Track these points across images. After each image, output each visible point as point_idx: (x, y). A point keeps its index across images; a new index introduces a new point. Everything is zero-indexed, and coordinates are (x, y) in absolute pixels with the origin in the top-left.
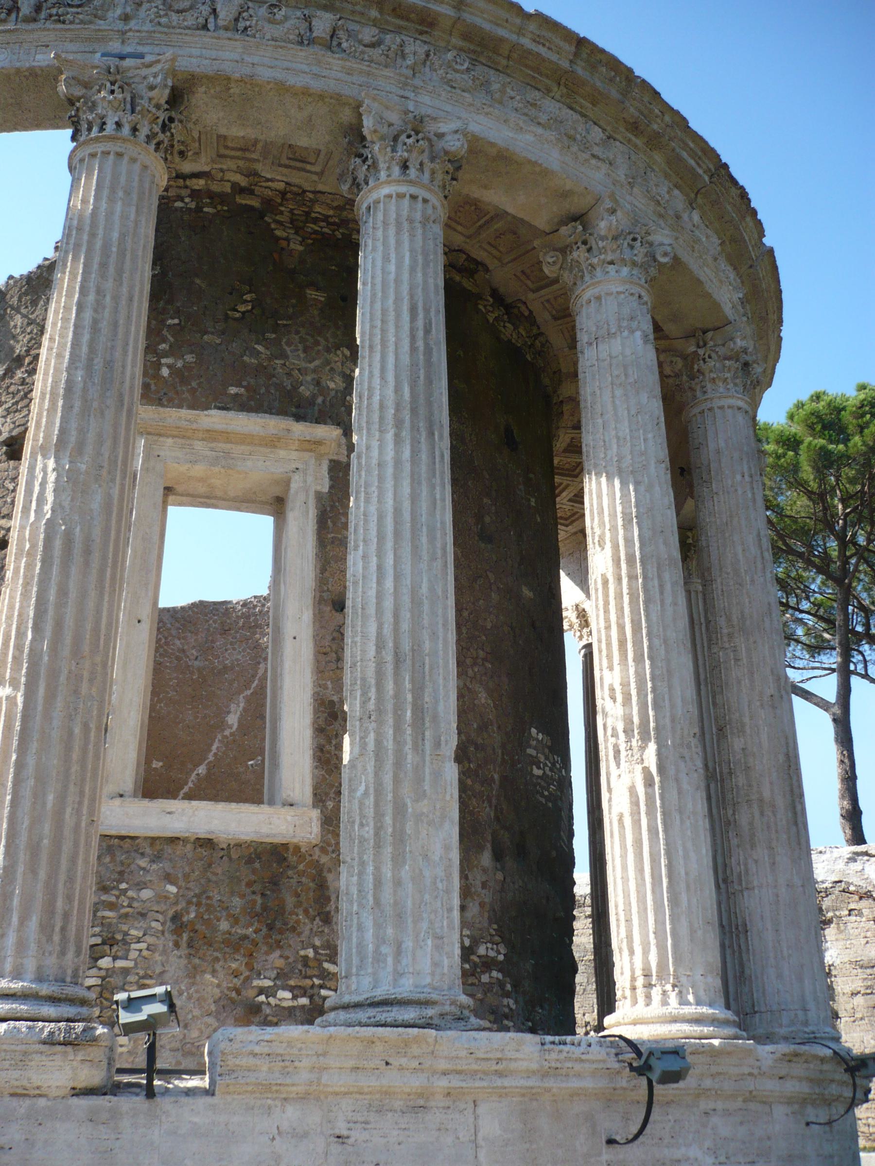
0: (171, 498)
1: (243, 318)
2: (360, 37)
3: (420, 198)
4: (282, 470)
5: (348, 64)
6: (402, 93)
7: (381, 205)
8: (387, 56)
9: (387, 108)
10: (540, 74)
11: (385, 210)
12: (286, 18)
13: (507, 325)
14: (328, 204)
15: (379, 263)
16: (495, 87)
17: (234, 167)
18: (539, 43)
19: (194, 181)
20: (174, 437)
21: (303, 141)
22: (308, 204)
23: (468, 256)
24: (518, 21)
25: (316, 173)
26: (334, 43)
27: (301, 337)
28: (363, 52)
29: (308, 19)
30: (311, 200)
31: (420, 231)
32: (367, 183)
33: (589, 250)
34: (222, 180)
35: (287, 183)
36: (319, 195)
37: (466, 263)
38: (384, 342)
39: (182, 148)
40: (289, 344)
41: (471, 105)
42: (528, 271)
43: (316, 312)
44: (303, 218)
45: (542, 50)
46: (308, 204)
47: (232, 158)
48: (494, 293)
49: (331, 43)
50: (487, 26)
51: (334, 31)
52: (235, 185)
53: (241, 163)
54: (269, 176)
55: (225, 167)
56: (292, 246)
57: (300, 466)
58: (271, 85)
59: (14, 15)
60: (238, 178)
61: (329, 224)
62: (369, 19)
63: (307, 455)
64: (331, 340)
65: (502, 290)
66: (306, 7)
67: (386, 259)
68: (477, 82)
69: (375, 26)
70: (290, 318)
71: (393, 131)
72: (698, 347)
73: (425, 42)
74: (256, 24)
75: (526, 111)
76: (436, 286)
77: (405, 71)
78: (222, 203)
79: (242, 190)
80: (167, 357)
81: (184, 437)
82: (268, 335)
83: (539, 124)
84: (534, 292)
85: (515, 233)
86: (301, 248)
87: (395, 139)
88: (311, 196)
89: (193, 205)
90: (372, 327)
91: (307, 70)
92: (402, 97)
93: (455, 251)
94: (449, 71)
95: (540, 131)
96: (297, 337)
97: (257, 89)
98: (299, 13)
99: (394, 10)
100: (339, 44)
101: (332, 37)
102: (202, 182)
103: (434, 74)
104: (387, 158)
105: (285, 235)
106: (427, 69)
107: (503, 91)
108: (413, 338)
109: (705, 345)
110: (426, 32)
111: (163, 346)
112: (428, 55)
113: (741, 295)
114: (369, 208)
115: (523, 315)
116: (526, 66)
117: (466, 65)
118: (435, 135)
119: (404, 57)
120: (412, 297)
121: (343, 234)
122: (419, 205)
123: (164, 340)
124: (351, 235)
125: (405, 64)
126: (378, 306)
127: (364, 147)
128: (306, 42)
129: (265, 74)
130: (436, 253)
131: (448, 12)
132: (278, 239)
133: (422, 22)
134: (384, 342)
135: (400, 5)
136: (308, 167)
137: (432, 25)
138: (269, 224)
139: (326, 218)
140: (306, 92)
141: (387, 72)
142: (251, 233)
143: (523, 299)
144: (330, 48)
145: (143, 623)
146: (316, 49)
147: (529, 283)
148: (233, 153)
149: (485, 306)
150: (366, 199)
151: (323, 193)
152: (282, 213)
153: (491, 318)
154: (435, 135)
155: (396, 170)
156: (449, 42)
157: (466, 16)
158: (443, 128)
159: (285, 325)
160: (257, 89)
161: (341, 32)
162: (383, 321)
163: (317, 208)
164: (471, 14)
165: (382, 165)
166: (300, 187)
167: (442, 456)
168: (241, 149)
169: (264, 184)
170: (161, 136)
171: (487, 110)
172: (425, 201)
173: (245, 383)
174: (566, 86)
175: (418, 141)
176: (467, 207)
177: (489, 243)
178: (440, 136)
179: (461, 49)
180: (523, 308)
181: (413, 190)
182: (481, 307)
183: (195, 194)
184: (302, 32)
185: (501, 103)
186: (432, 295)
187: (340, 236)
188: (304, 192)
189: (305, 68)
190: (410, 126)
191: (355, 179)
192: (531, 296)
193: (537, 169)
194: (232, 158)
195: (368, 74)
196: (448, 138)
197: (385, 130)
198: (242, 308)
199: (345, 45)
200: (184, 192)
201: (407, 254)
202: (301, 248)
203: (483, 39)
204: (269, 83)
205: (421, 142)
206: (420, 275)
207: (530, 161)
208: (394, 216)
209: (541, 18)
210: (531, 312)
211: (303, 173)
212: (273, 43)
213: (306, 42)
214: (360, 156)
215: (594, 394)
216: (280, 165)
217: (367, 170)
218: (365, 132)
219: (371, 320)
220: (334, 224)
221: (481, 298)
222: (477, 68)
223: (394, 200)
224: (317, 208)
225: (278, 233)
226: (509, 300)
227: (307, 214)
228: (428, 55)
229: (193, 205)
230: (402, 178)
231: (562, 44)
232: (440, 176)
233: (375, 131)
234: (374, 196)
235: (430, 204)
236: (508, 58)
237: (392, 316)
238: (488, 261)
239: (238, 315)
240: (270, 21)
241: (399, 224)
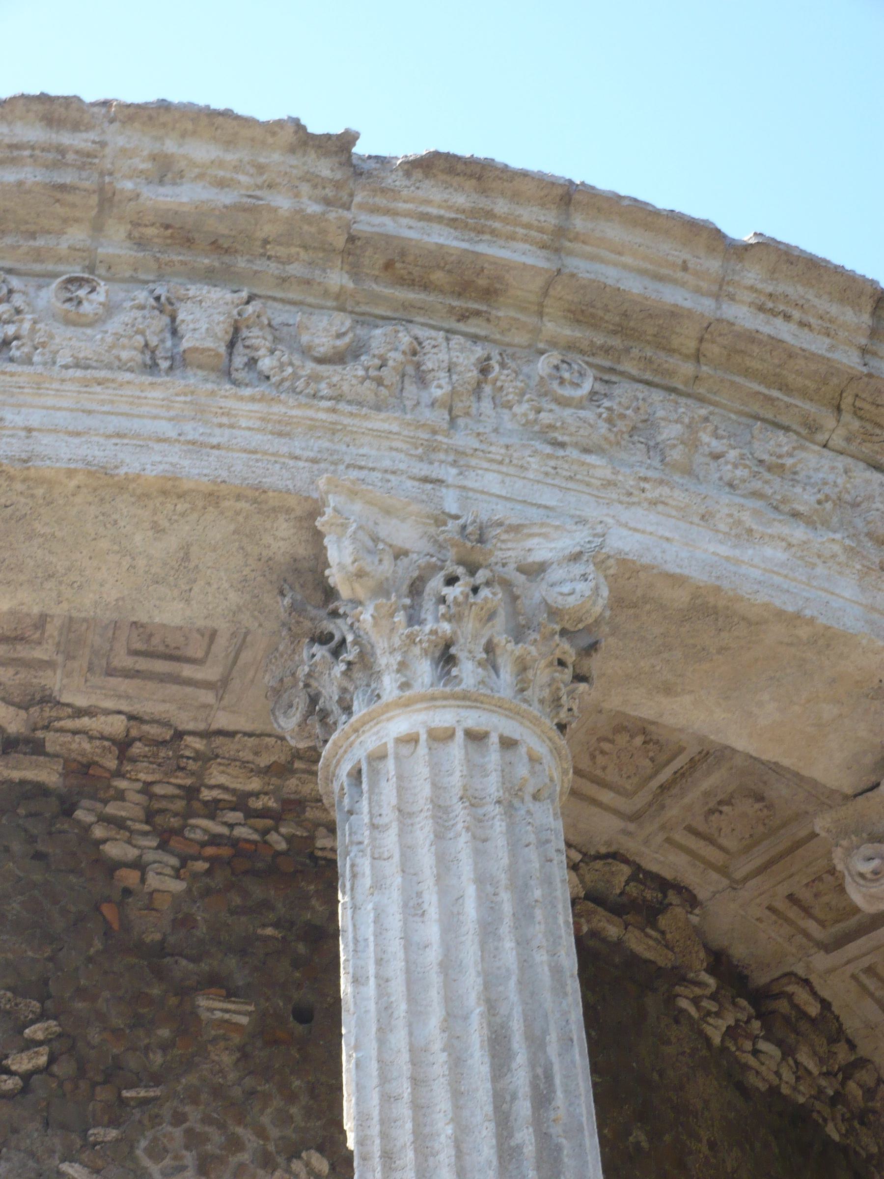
1: (25, 1090)
2: (305, 339)
3: (494, 739)
5: (278, 409)
6: (424, 469)
7: (390, 764)
8: (380, 382)
9: (388, 512)
10: (785, 387)
11: (400, 777)
12: (110, 309)
13: (763, 1046)
14: (244, 763)
15: (394, 921)
16: (670, 432)
18: (773, 313)
21: (169, 613)
22: (192, 765)
23: (638, 868)
24: (714, 265)
25: (207, 685)
26: (239, 361)
27: (189, 1132)
28: (315, 378)
29: (166, 307)
30: (198, 756)
31: (499, 826)
32: (348, 709)
35: (131, 717)
36: (219, 740)
37: (633, 890)
38: (422, 1139)
40: (156, 1152)
41: (609, 484)
42: (805, 895)
43: (227, 1059)
44: (179, 805)
45: (785, 331)
46: (192, 765)
48: (719, 962)
49: (232, 358)
50: (634, 285)
51: (237, 330)
54: (81, 701)
56: (153, 881)
58: (79, 479)
61: (251, 814)
62: (326, 293)
64: (274, 1132)
65: (739, 952)
66: (160, 277)
67: (413, 908)
68: (621, 425)
69: (342, 309)
70: (156, 1079)
71: (407, 570)
73: (475, 338)
74: (33, 331)
75: (757, 485)
76: (556, 971)
77: (429, 415)
82: (97, 1133)
83: (795, 515)
84: (827, 948)
85: (760, 798)
86: (178, 886)
87: (416, 589)
88: (198, 744)
90: (388, 1099)
91: (173, 434)
92: (426, 480)
93: (599, 857)
94: (546, 404)
95: (799, 533)
96: (178, 1133)
97: (40, 492)
98: (142, 296)
99: (388, 266)
100: (252, 362)
101: (231, 345)
103: (506, 414)
104: (397, 642)
105: (132, 853)
106: (486, 405)
107: (693, 444)
108: (503, 1121)
110: (478, 313)
112: (484, 370)
114: (356, 775)
115: (803, 1015)
116: (747, 373)
117: (587, 385)
118: (521, 569)
119: (422, 380)
120: (491, 1005)
121: (290, 839)
122: (493, 756)
124: (312, 838)
125: (425, 397)
126: (399, 1039)
127: (334, 614)
128: (164, 364)
129: (60, 451)
130: (548, 881)
131: (530, 261)
132: (112, 867)
133: (463, 289)
134: (422, 1139)
135: (403, 254)
136: (187, 671)
137: (489, 294)
138: (87, 828)
139: (241, 802)
140: (170, 489)
141: (380, 422)
142: (39, 856)
143: (801, 972)
144: (227, 373)
146: (193, 379)
147: (811, 926)
149: (696, 1001)
150: (348, 749)
151: (231, 734)
152: (120, 796)
153: (715, 1032)
154: (521, 569)
155: (424, 670)
156: (536, 331)
157: (575, 264)
158: (541, 550)
159: (144, 1102)
160: (40, 492)
161: (256, 332)
162: (416, 1082)
163: (217, 776)
164: (593, 258)
165: (385, 660)
166: (167, 724)
169: (69, 724)
171: (653, 493)
172: (508, 744)
174: (857, 412)
175: (475, 590)
176: (622, 739)
178: (535, 571)
179: (571, 347)
180: (802, 996)
181: (473, 719)
182: (684, 1003)
184: (154, 341)
185: (688, 471)
186: (547, 999)
187: (283, 846)
188: (179, 735)
189: (167, 429)
190: (451, 554)
191: (314, 700)
192: (821, 961)
193: (803, 632)
195: (333, 430)
196: (555, 574)
197: (386, 568)
198: (22, 1063)
199: (266, 363)
201: (471, 891)
202: (178, 886)
203: (625, 315)
204: (71, 473)
205: (485, 592)
206: (509, 944)
207: (780, 614)
208: (426, 790)
209: (773, 253)
210: (825, 1005)
211: (175, 688)
212: (79, 373)
213: (164, 364)
214: (324, 639)
216: (111, 672)
217: (347, 673)
218: (335, 577)
219: (384, 1079)
220: (264, 813)
221: (683, 980)
222: (617, 391)
223: (422, 750)
224: (217, 776)
225: (114, 850)
226: (761, 979)
227: (191, 793)
228: (484, 370)
230: (440, 688)
231: (835, 310)
232: (541, 674)
233: (360, 574)
234: (369, 742)
235: (523, 750)
236: (697, 357)
237: (439, 1061)
240: (68, 322)
241: (440, 811)
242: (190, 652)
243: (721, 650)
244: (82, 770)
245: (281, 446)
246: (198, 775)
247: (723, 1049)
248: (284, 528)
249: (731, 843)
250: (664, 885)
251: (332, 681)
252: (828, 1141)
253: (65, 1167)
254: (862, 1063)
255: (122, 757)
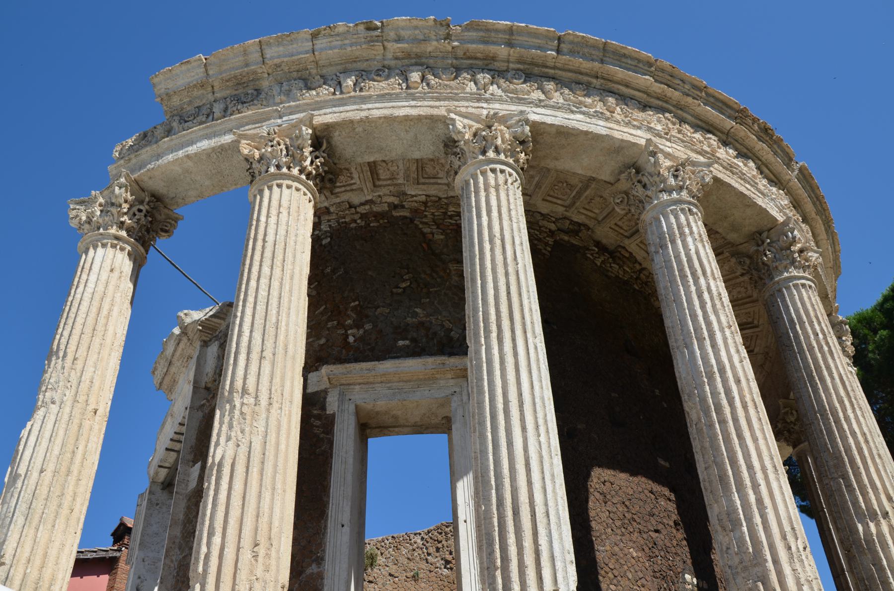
0: (368, 431)
4: (443, 395)
17: (388, 192)
19: (362, 207)
20: (360, 384)
30: (446, 204)
33: (645, 186)
34: (381, 203)
37: (571, 227)
39: (331, 176)
42: (620, 223)
47: (385, 186)
48: (598, 244)
52: (389, 204)
53: (391, 188)
54: (413, 193)
55: (381, 194)
57: (457, 390)
59: (211, 117)
60: (391, 199)
63: (460, 380)
65: (604, 241)
72: (758, 245)
78: (383, 218)
79: (396, 207)
80: (352, 329)
81: (367, 383)
84: (628, 238)
85: (601, 197)
86: (442, 237)
89: (363, 224)
102: (367, 207)
109: (763, 242)
111: (349, 322)
113: (786, 202)
123: (349, 317)
136: (439, 181)
138: (417, 226)
145: (345, 527)
148: (385, 183)
149: (592, 255)
152: (426, 216)
159: (436, 292)
167: (536, 348)
168: (390, 179)
170: (310, 168)
173: (409, 337)
176: (560, 185)
177: (584, 208)
180: (623, 252)
183: (363, 216)
188: (440, 199)
192: (627, 242)
194: (385, 186)
198: (404, 285)
200: (356, 217)
210: (631, 254)
215: (666, 288)
216: (418, 183)
221: (588, 249)
226: (612, 248)
227: (445, 213)
229: (363, 224)
238: (587, 222)
239: (400, 290)
242: (439, 176)
243: (568, 144)
244: (415, 211)
245: (437, 103)
246: (447, 209)
247: (601, 266)
248: (441, 126)
249: (597, 211)
250: (579, 224)
251: (457, 163)
252: (635, 289)
253: (416, 310)
254: (644, 269)
255: (426, 207)
